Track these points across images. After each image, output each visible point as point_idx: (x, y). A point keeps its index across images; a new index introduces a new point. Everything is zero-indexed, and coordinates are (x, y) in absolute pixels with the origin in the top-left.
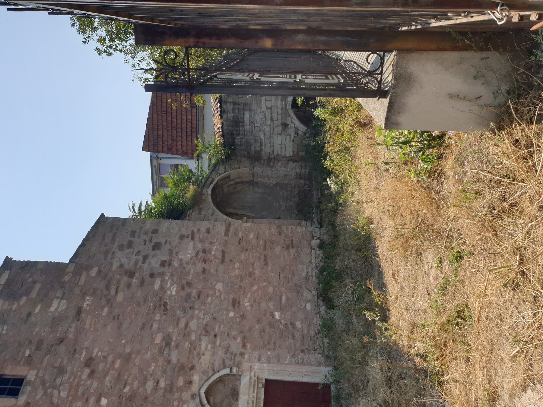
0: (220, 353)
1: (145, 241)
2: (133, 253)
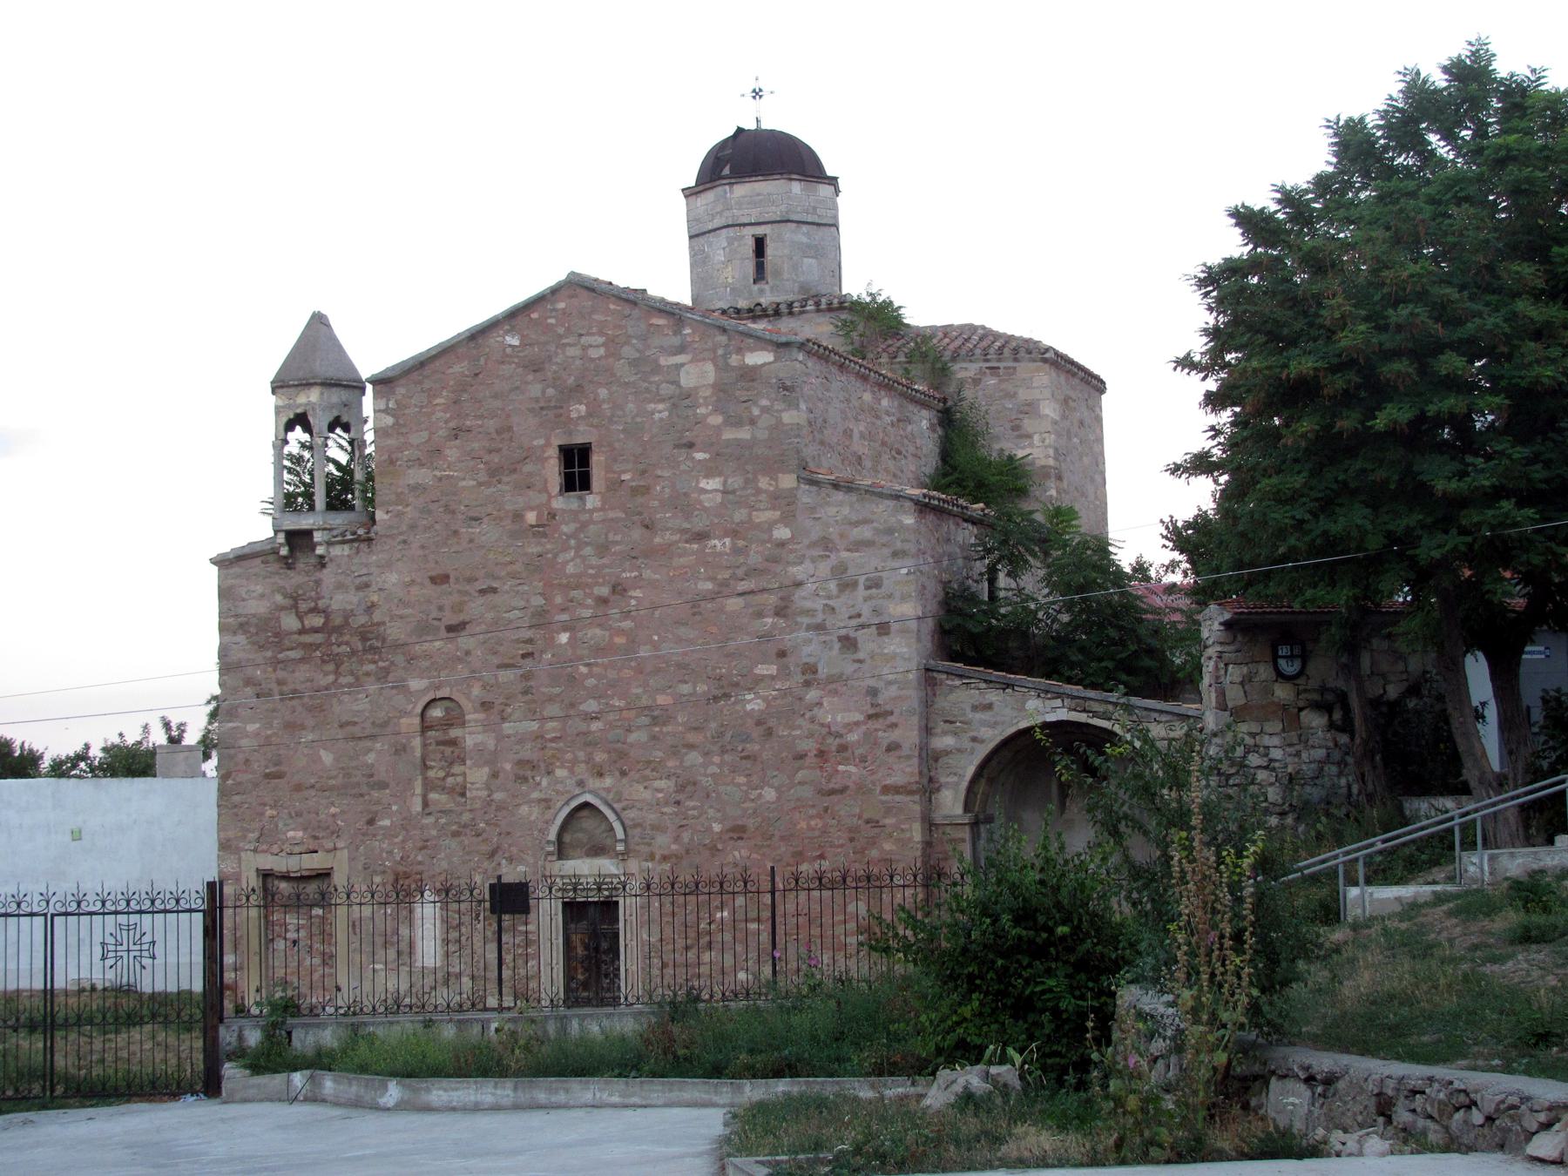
0: (652, 816)
1: (859, 616)
2: (829, 598)
